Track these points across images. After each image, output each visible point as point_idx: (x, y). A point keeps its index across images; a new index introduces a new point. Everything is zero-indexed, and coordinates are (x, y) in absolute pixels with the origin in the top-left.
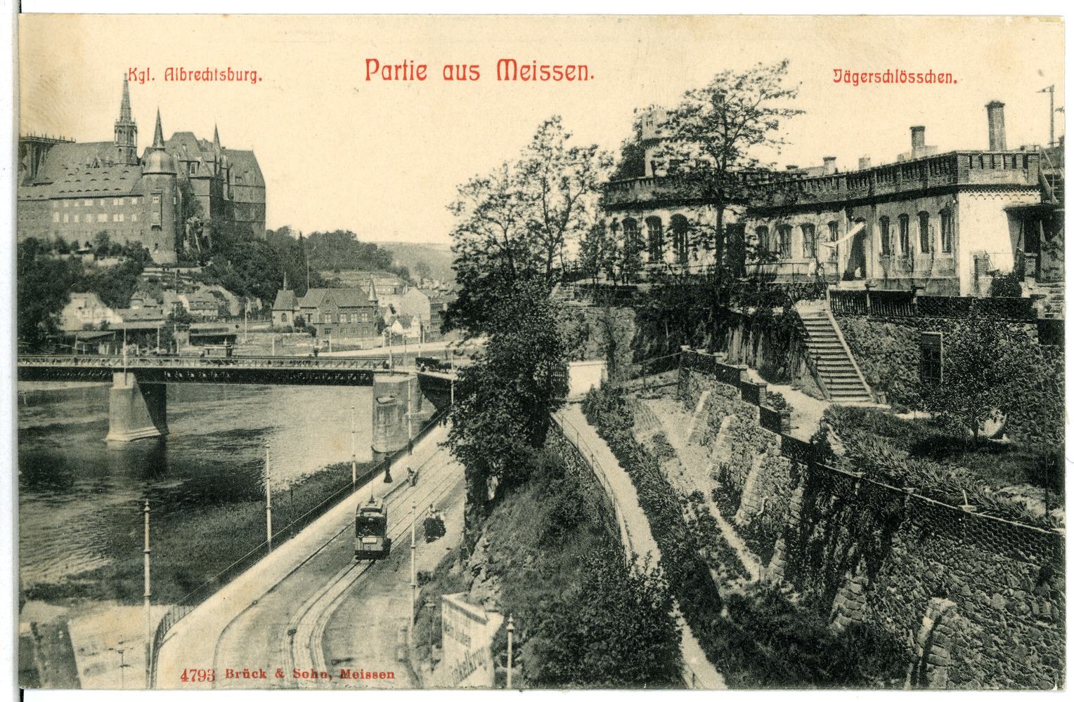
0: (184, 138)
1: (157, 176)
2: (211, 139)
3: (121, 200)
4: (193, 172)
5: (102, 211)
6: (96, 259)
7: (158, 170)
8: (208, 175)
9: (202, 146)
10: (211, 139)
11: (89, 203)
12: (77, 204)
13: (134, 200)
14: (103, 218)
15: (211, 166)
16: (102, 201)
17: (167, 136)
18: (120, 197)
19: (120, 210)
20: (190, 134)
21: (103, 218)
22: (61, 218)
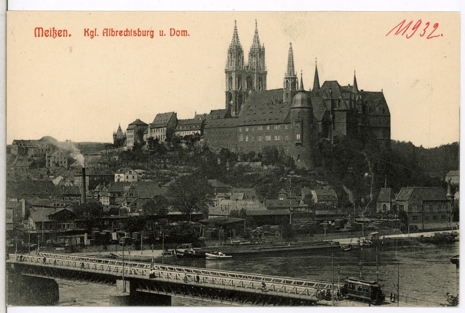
0: (332, 85)
1: (298, 109)
2: (352, 84)
3: (279, 126)
5: (268, 133)
6: (262, 165)
7: (299, 105)
8: (346, 109)
9: (344, 90)
10: (352, 84)
11: (261, 128)
12: (253, 129)
13: (286, 127)
14: (269, 138)
15: (348, 102)
16: (268, 128)
17: (321, 84)
18: (278, 124)
19: (278, 133)
21: (269, 138)
22: (244, 140)
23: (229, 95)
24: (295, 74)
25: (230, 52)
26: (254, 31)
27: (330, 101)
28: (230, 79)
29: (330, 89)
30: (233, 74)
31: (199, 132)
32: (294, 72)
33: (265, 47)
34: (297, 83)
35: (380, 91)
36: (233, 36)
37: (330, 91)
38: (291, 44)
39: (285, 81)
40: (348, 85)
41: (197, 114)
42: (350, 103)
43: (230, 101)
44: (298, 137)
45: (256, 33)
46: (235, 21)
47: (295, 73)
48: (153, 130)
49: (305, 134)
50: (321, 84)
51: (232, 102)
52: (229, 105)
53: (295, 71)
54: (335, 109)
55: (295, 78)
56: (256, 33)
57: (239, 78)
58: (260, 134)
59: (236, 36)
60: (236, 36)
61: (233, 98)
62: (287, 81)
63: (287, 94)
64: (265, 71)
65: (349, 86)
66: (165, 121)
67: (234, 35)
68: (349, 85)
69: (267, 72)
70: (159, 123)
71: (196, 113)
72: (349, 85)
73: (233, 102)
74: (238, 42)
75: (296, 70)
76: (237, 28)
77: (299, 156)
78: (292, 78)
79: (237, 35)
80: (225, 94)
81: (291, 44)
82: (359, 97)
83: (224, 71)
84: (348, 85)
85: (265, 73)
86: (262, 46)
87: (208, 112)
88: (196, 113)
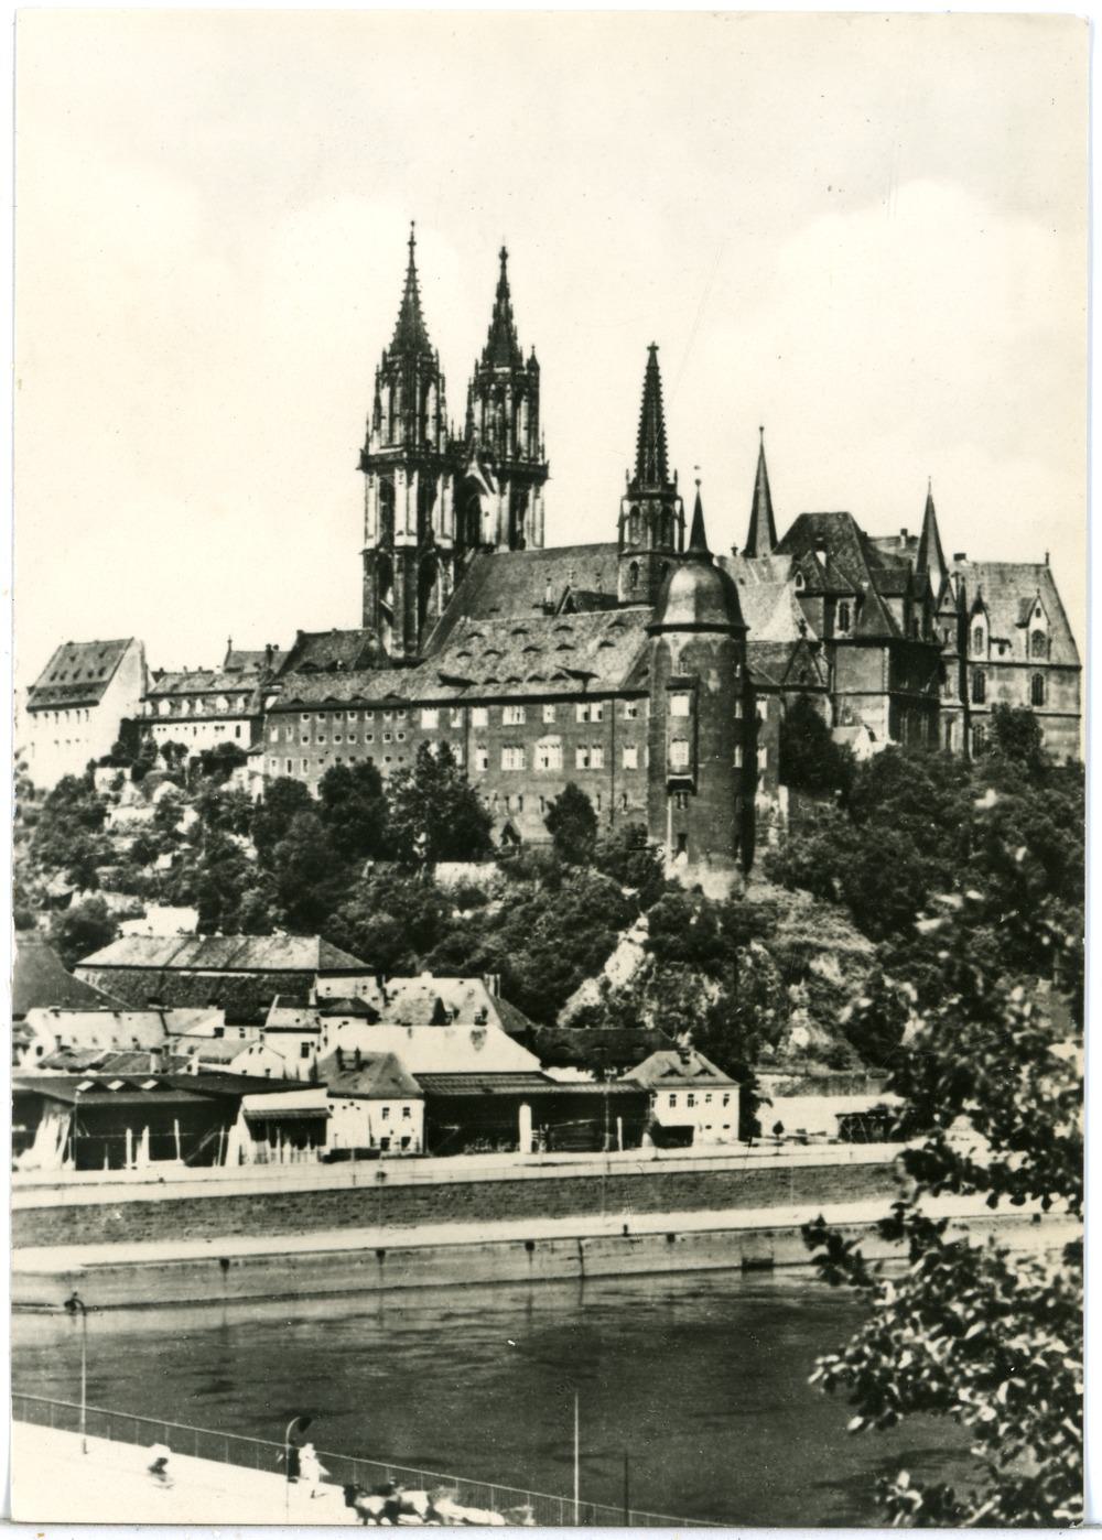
1: (685, 638)
3: (596, 707)
4: (844, 626)
11: (511, 716)
15: (897, 607)
16: (548, 713)
20: (846, 516)
23: (378, 564)
24: (671, 481)
25: (386, 375)
26: (493, 290)
27: (821, 600)
28: (387, 494)
29: (822, 547)
30: (397, 473)
31: (246, 726)
32: (663, 470)
33: (540, 360)
34: (676, 523)
35: (1043, 561)
36: (399, 307)
37: (822, 556)
38: (653, 349)
39: (627, 507)
40: (898, 533)
41: (234, 648)
42: (908, 610)
43: (383, 595)
44: (678, 755)
45: (503, 291)
46: (412, 243)
47: (670, 475)
48: (41, 714)
49: (706, 744)
50: (782, 529)
51: (390, 597)
52: (377, 615)
53: (671, 467)
54: (838, 634)
55: (670, 494)
56: (503, 291)
57: (426, 499)
58: (514, 740)
59: (410, 313)
60: (410, 313)
61: (399, 577)
62: (635, 511)
63: (634, 566)
64: (540, 463)
65: (903, 538)
66: (95, 679)
67: (405, 303)
68: (904, 532)
69: (545, 467)
70: (68, 681)
71: (230, 642)
72: (904, 532)
75: (673, 462)
76: (418, 275)
78: (652, 497)
79: (417, 302)
80: (360, 561)
81: (653, 349)
82: (945, 585)
83: (356, 460)
84: (898, 533)
86: (526, 356)
87: (287, 644)
88: (230, 642)
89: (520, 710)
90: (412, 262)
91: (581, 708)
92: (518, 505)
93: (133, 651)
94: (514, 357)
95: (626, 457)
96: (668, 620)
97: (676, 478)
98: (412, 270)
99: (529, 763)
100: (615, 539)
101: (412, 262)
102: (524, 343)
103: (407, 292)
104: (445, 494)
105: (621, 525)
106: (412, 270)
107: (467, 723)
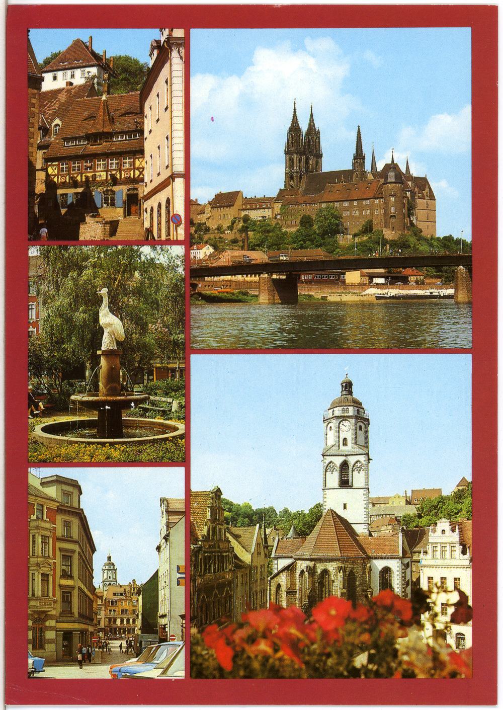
3: (368, 202)
11: (346, 204)
16: (355, 203)
28: (292, 160)
38: (359, 127)
43: (291, 181)
44: (393, 210)
45: (312, 115)
46: (295, 104)
56: (312, 115)
57: (300, 161)
62: (357, 162)
67: (294, 117)
69: (322, 154)
73: (294, 183)
74: (297, 122)
77: (393, 227)
81: (359, 127)
85: (321, 156)
89: (348, 203)
90: (295, 108)
91: (364, 202)
92: (317, 163)
93: (240, 194)
94: (315, 129)
95: (353, 151)
96: (389, 181)
97: (365, 155)
98: (295, 110)
99: (351, 213)
100: (352, 169)
101: (295, 108)
102: (316, 126)
103: (294, 114)
104: (304, 158)
105: (353, 165)
106: (295, 110)
107: (334, 206)
